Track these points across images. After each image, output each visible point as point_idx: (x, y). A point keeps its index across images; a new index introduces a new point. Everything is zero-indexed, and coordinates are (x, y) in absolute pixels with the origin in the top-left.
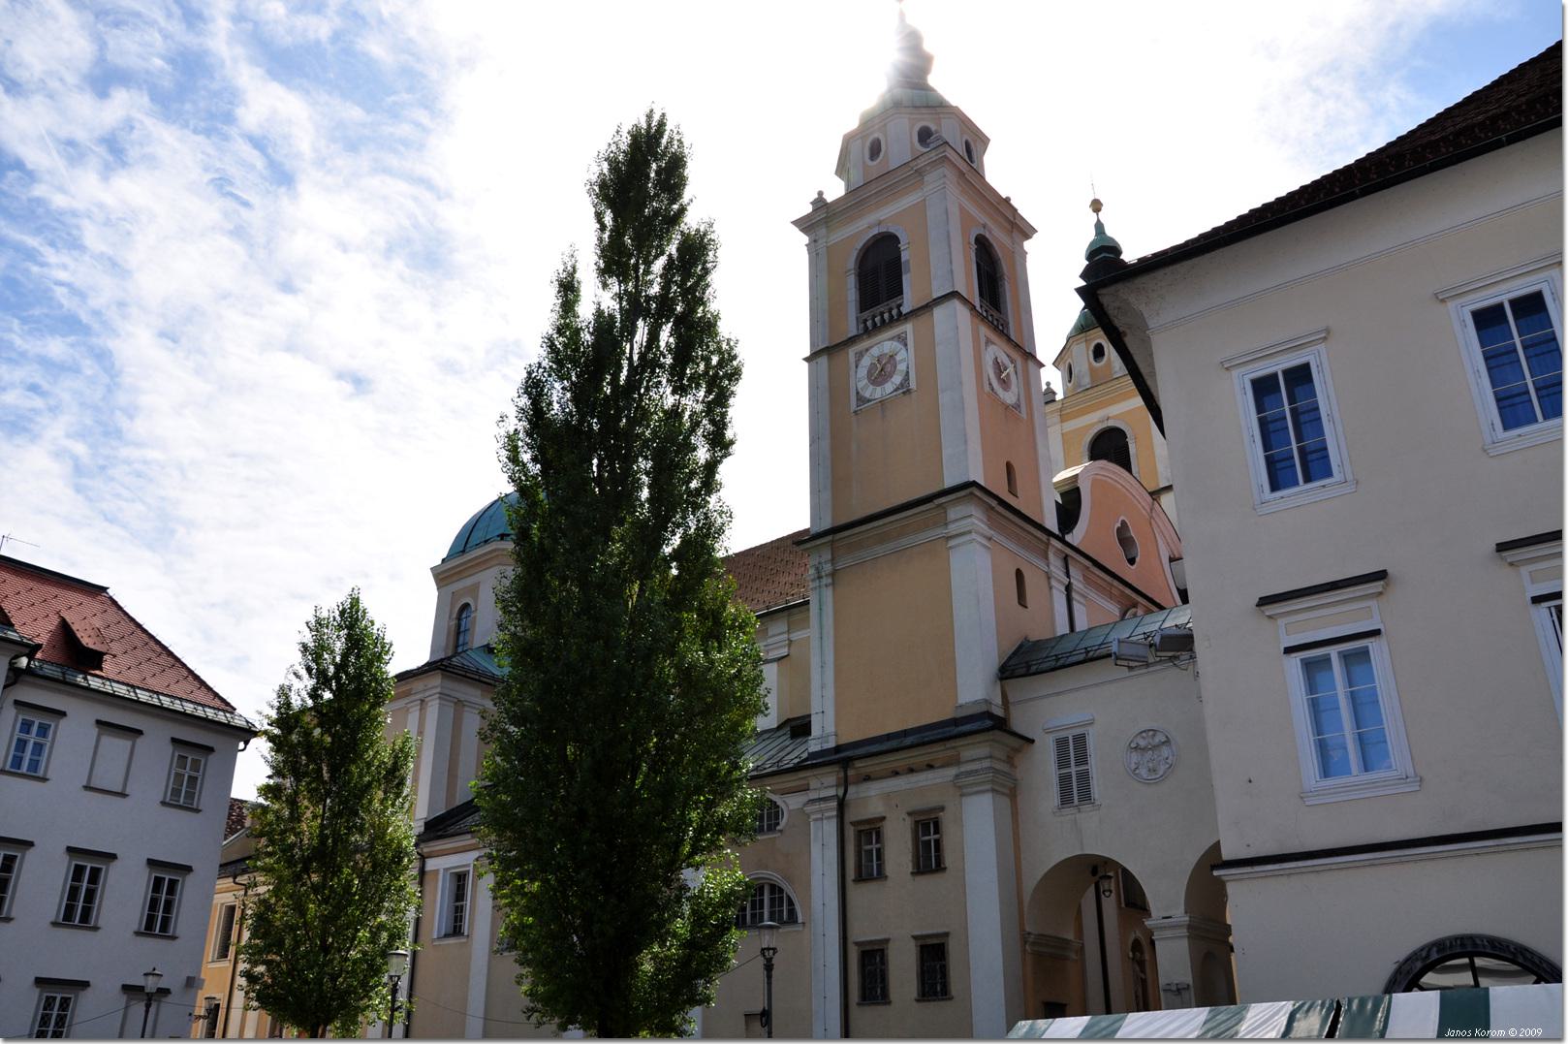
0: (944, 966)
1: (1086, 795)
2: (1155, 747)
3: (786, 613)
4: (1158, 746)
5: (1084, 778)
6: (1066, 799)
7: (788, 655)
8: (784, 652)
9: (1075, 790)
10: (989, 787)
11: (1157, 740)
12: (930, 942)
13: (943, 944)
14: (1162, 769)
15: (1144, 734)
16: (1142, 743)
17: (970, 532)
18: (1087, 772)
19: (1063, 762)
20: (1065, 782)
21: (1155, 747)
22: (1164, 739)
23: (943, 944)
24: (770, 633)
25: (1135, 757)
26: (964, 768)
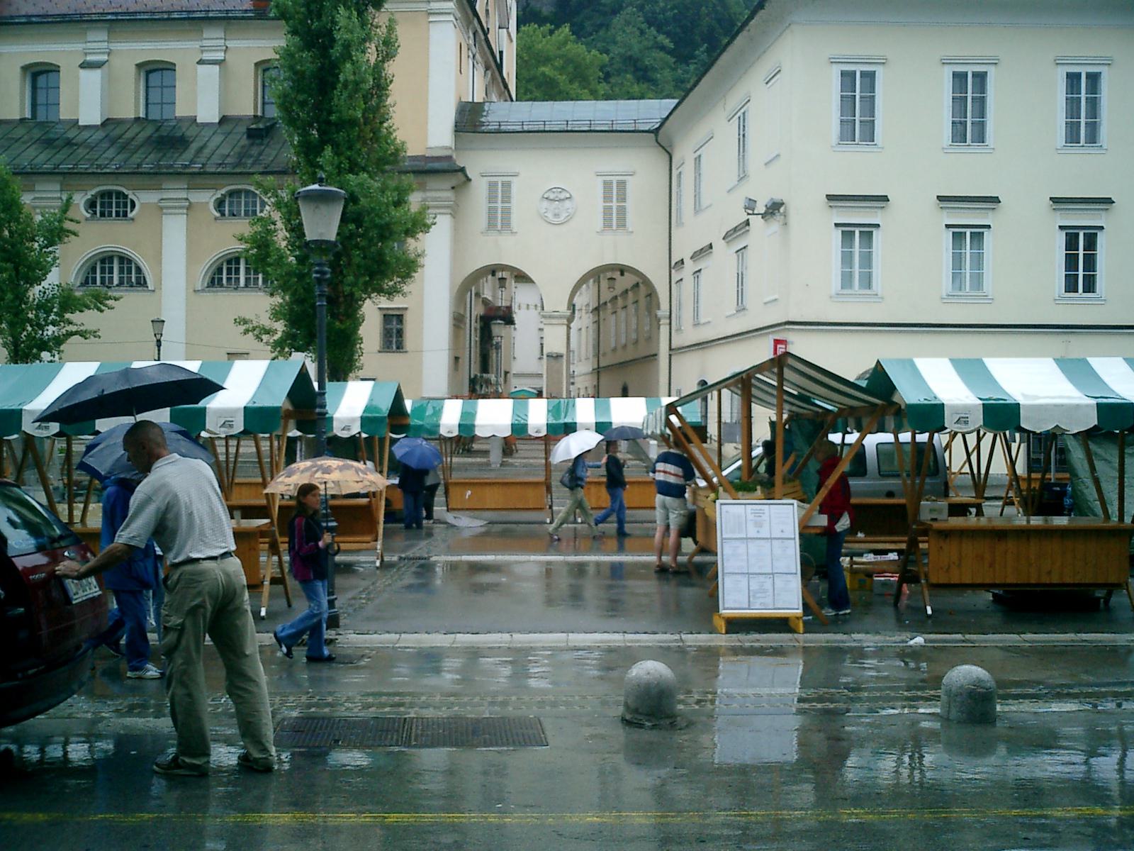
0: (401, 329)
1: (507, 224)
2: (560, 200)
3: (224, 23)
4: (563, 200)
5: (507, 212)
6: (491, 225)
7: (224, 60)
8: (220, 56)
9: (499, 221)
10: (448, 211)
11: (563, 196)
12: (391, 312)
13: (402, 315)
14: (564, 215)
15: (554, 190)
16: (552, 196)
17: (449, 13)
18: (509, 208)
19: (492, 198)
20: (492, 213)
21: (560, 200)
22: (568, 196)
23: (402, 315)
24: (205, 36)
25: (546, 204)
26: (429, 194)
